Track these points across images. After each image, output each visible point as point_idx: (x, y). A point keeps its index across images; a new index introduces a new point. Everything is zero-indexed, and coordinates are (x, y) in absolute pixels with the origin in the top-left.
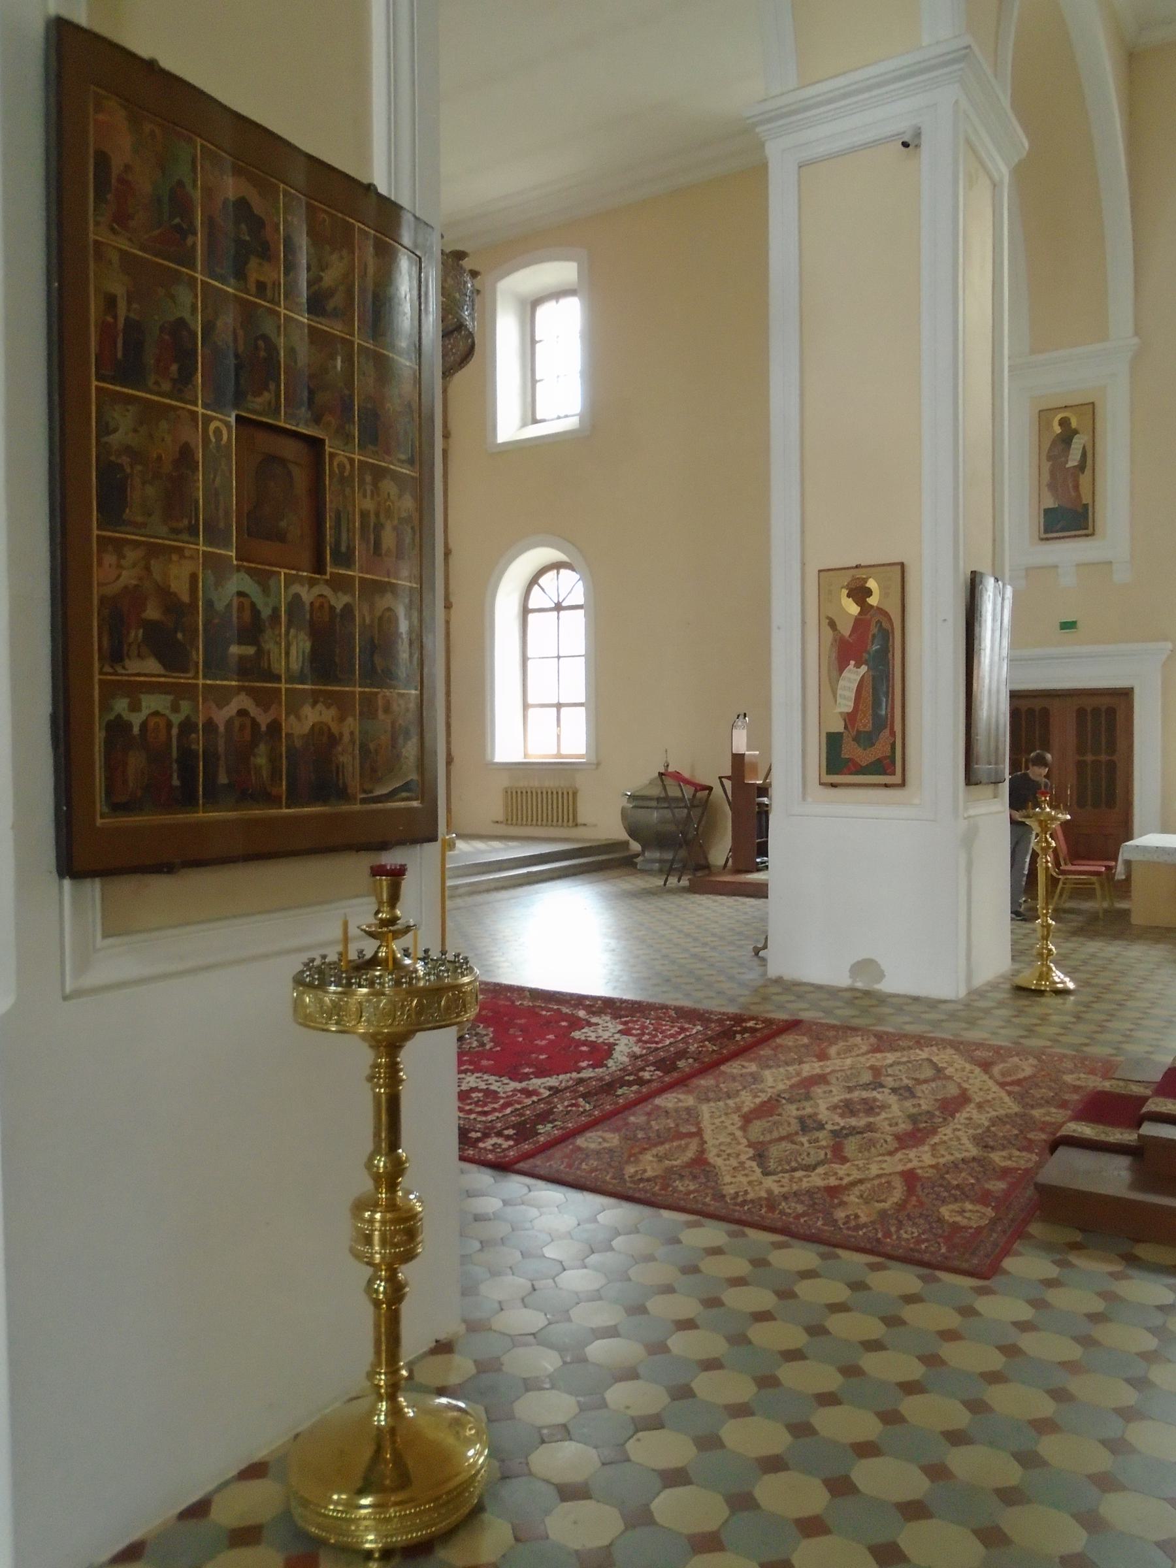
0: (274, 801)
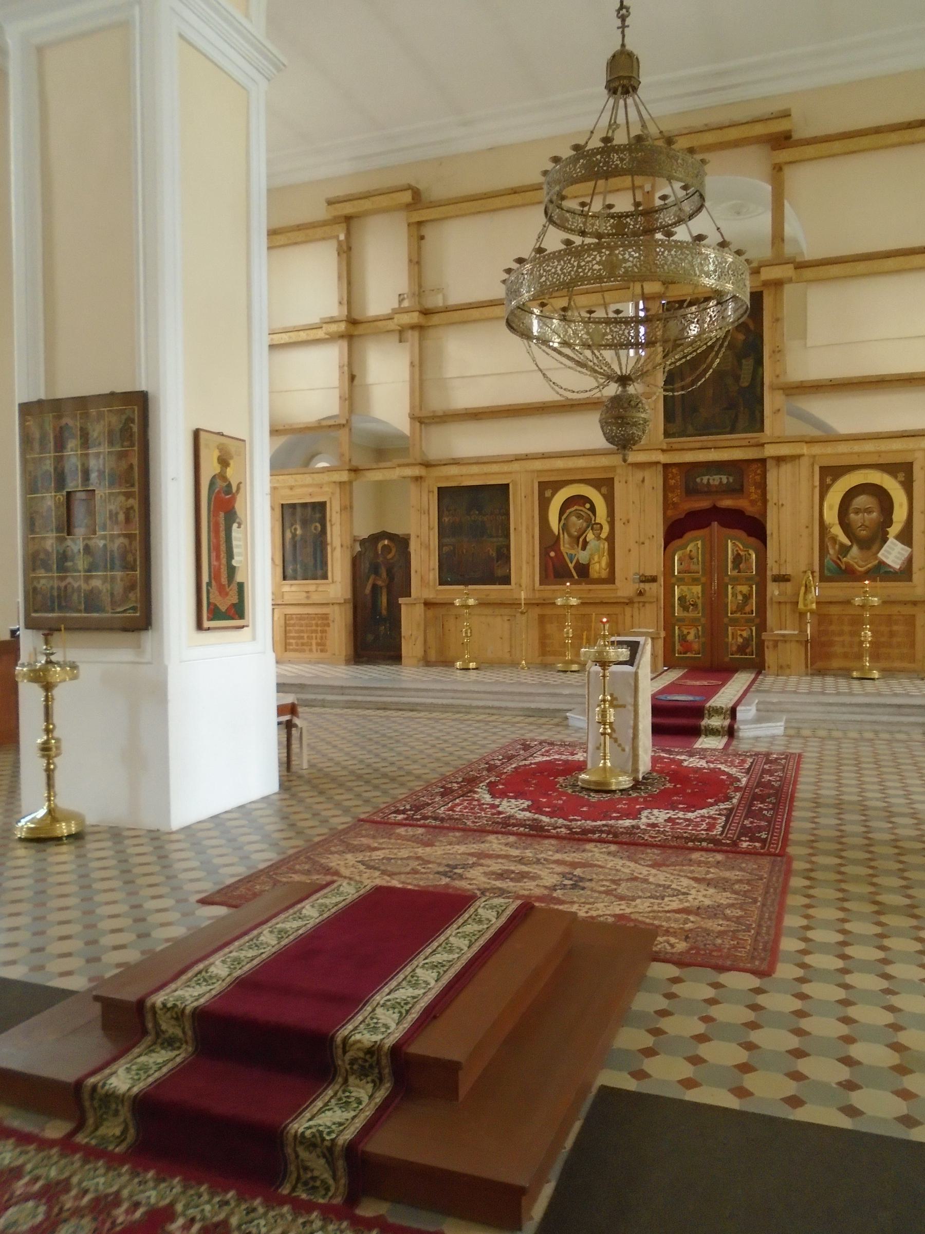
0: (79, 611)
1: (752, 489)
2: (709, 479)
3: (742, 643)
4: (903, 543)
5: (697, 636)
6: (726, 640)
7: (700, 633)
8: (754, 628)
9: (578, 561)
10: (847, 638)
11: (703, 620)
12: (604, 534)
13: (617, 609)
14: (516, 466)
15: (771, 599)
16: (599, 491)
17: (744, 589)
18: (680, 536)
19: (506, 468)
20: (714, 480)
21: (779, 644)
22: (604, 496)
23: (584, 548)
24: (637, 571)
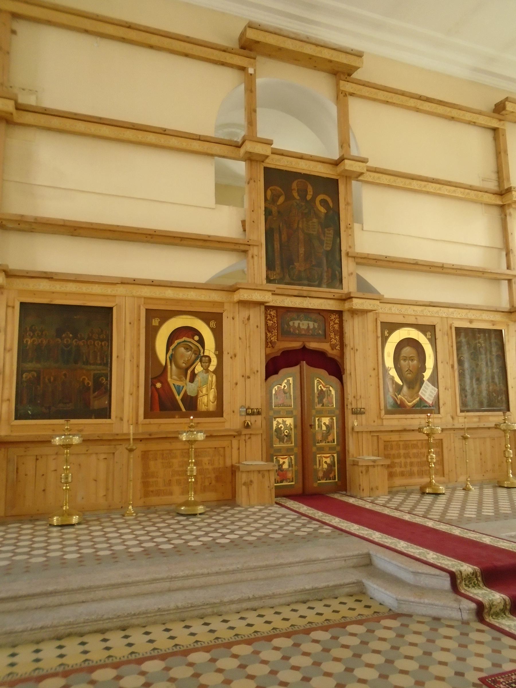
1: (332, 336)
2: (299, 324)
3: (327, 469)
4: (433, 385)
5: (290, 465)
6: (315, 467)
7: (293, 462)
8: (335, 455)
9: (186, 392)
10: (403, 460)
11: (296, 450)
12: (212, 367)
13: (225, 443)
14: (121, 290)
15: (353, 428)
16: (208, 325)
17: (326, 420)
18: (276, 373)
19: (109, 290)
20: (303, 324)
21: (371, 469)
22: (212, 330)
23: (192, 380)
24: (244, 405)
